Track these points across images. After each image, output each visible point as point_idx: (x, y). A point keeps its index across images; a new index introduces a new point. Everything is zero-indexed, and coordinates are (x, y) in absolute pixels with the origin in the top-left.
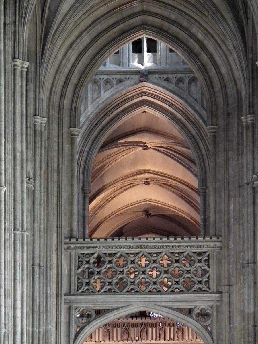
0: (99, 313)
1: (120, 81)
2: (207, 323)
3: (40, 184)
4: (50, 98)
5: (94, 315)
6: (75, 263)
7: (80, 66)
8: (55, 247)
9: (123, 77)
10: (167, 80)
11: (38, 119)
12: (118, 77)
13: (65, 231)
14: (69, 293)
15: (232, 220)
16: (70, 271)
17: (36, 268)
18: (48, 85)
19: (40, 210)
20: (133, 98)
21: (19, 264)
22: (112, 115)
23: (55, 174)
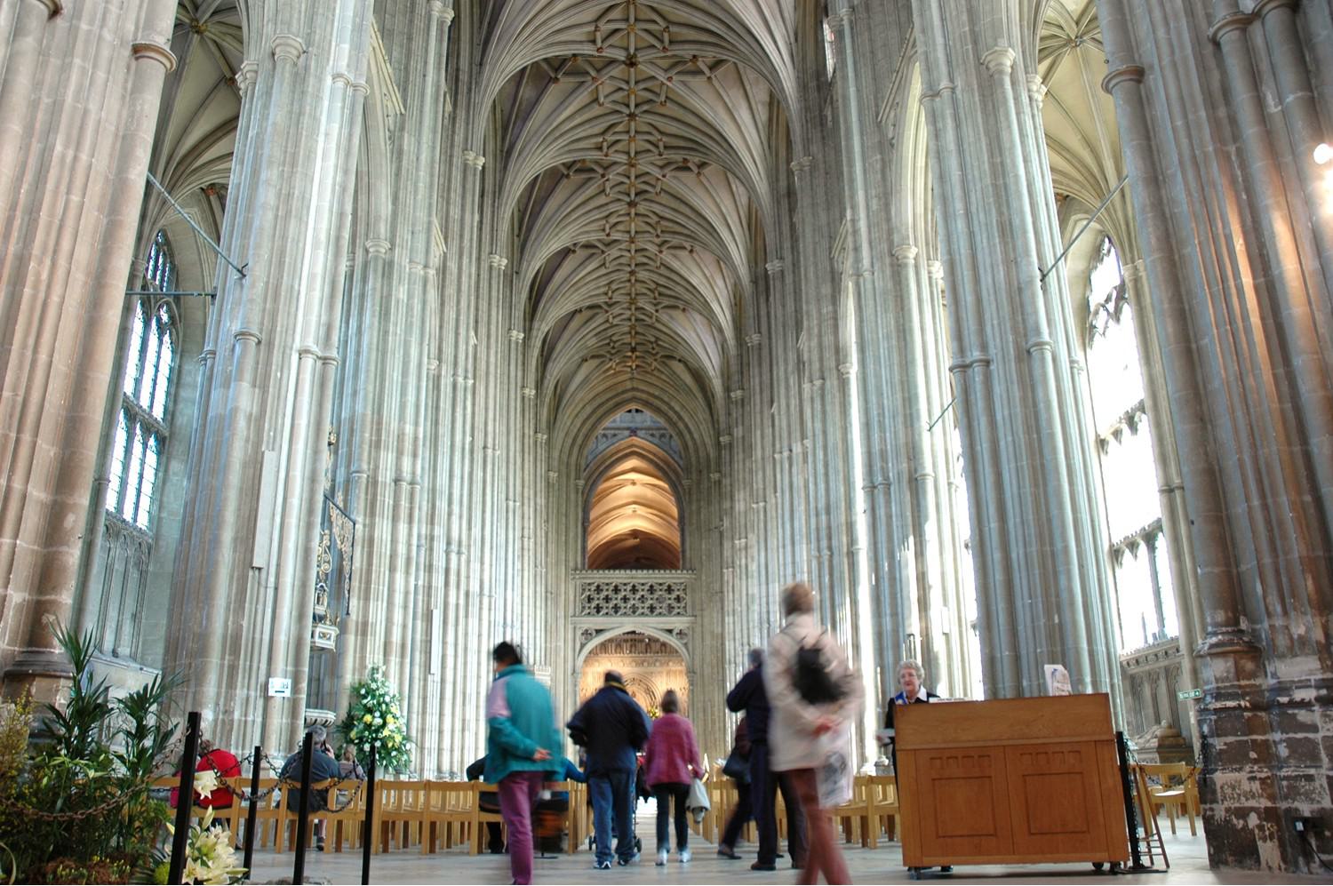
0: (599, 632)
1: (615, 435)
2: (685, 641)
3: (553, 522)
4: (560, 457)
5: (594, 634)
6: (579, 590)
7: (584, 430)
8: (563, 577)
9: (616, 432)
10: (652, 435)
11: (551, 474)
12: (612, 432)
13: (571, 564)
14: (574, 616)
15: (704, 557)
16: (575, 597)
17: (549, 595)
18: (559, 446)
19: (552, 547)
20: (624, 449)
21: (538, 595)
22: (607, 463)
23: (564, 518)
